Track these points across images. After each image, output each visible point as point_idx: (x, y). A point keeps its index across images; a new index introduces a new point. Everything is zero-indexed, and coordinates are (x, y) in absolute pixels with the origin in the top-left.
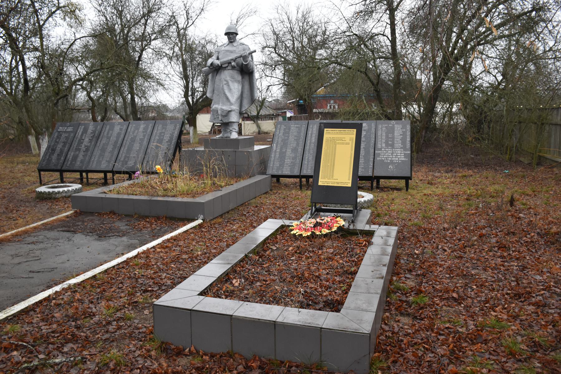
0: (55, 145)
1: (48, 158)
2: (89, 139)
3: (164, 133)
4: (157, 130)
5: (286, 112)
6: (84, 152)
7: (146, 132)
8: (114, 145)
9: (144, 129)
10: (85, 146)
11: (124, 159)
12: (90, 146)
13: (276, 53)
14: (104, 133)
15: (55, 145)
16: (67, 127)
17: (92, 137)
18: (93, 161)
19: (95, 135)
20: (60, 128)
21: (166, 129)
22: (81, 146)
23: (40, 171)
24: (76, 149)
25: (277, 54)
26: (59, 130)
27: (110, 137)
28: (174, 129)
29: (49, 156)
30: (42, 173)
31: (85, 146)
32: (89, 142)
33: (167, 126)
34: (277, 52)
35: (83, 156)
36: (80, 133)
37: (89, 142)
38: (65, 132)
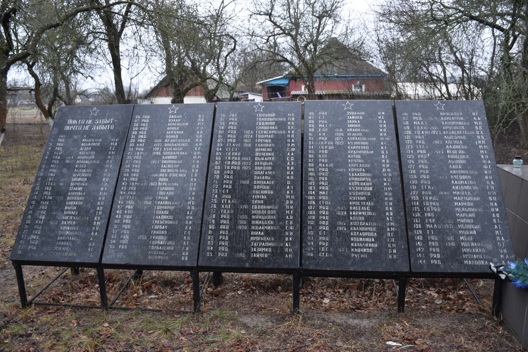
0: (63, 175)
1: (46, 223)
2: (180, 158)
3: (440, 137)
4: (412, 129)
5: (247, 95)
6: (171, 199)
7: (376, 133)
8: (273, 177)
9: (364, 124)
10: (171, 180)
11: (333, 226)
12: (186, 180)
13: (271, 20)
14: (225, 137)
15: (63, 175)
16: (94, 118)
17: (184, 149)
18: (217, 230)
19: (191, 145)
20: (70, 121)
21: (440, 127)
22: (156, 179)
23: (18, 265)
24: (139, 189)
25: (273, 22)
26: (67, 128)
27: (252, 150)
28: (471, 127)
29: (49, 210)
30: (26, 270)
31: (171, 180)
32: (181, 166)
33: (439, 116)
34: (272, 19)
35: (171, 213)
36: (142, 138)
37: (181, 166)
38: (89, 134)
